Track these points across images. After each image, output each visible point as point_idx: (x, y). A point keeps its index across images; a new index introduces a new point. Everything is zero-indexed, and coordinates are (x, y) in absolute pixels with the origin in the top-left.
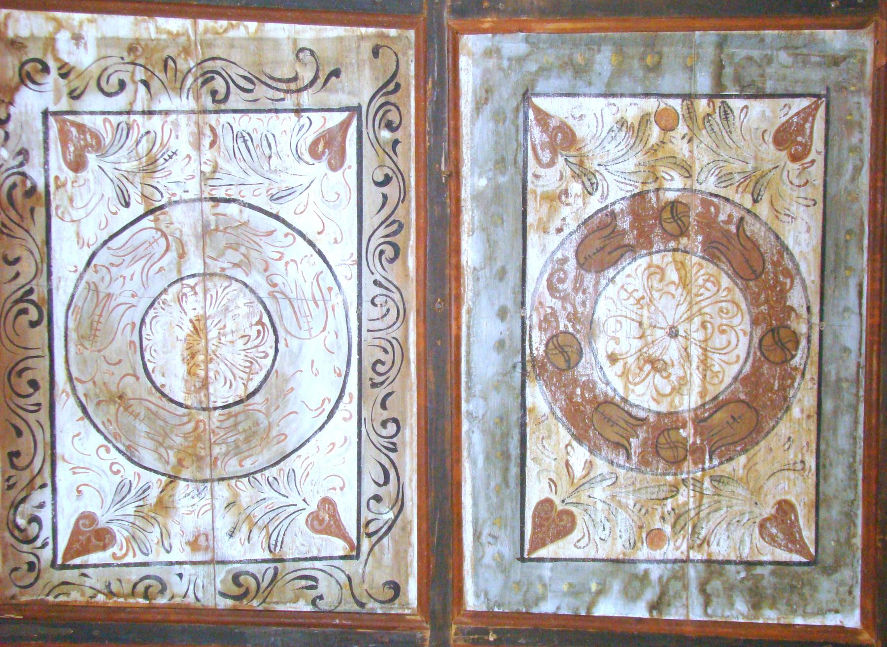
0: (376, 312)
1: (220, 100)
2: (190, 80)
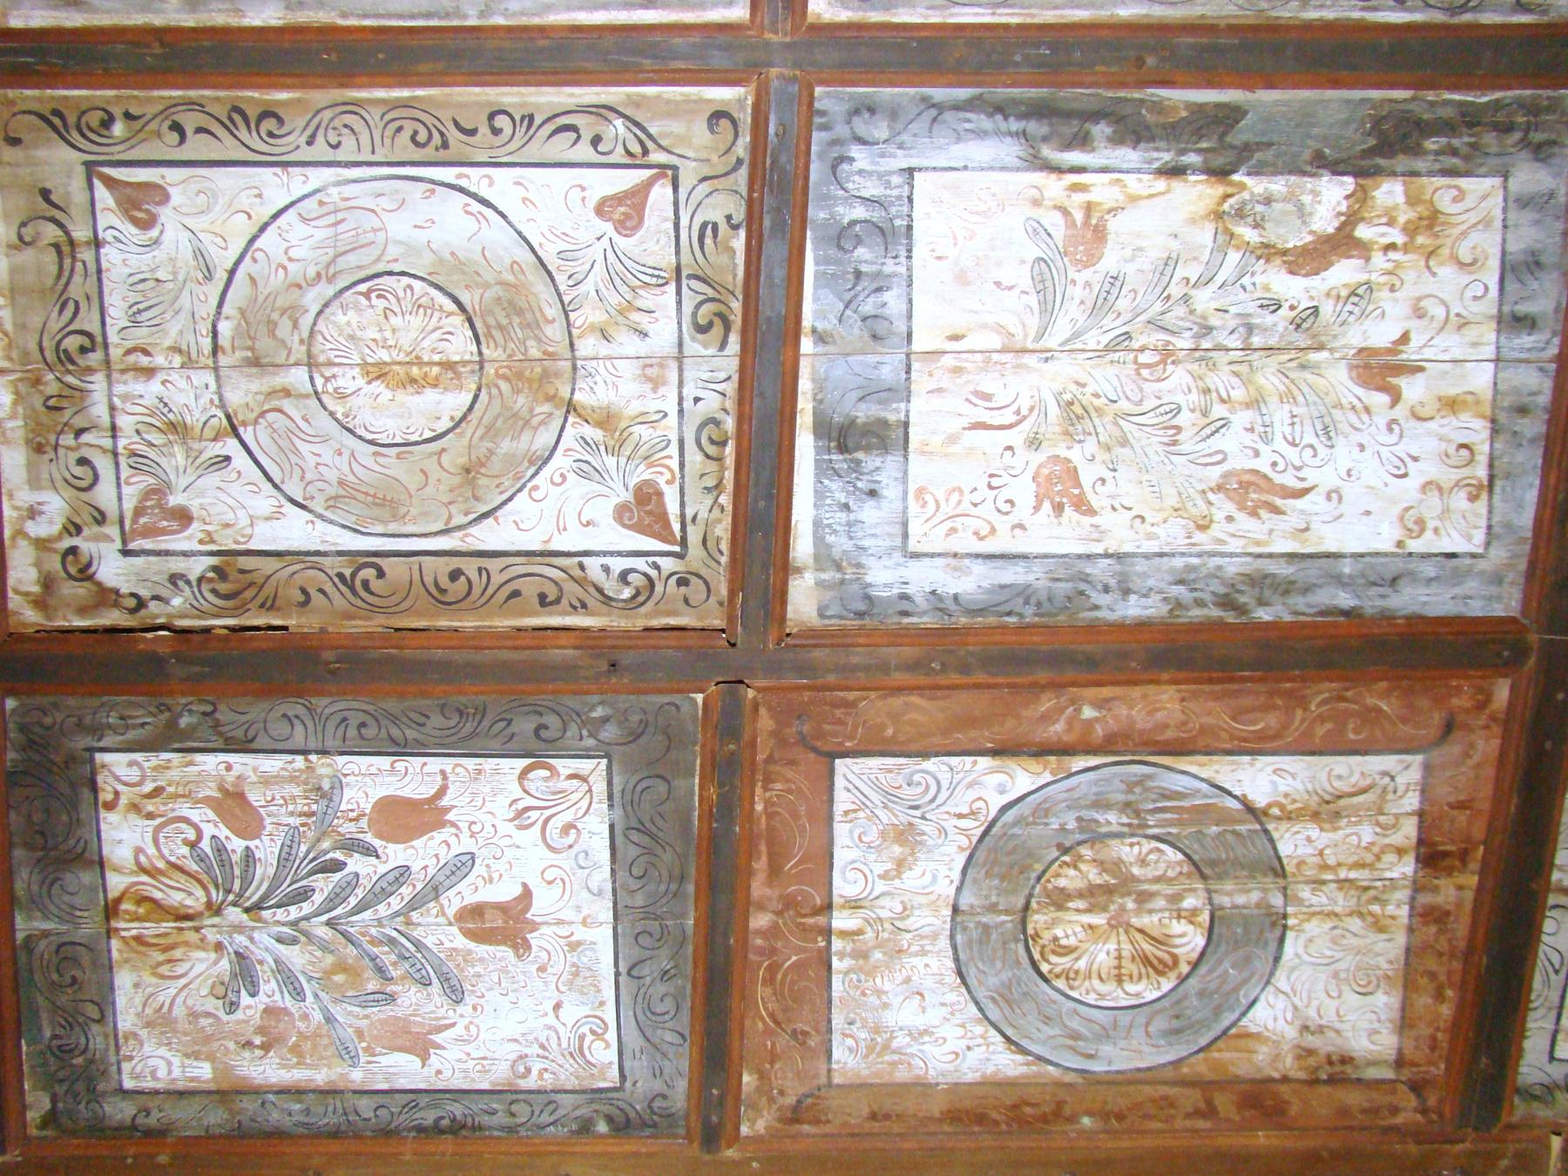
0: (348, 142)
1: (92, 343)
2: (70, 379)
